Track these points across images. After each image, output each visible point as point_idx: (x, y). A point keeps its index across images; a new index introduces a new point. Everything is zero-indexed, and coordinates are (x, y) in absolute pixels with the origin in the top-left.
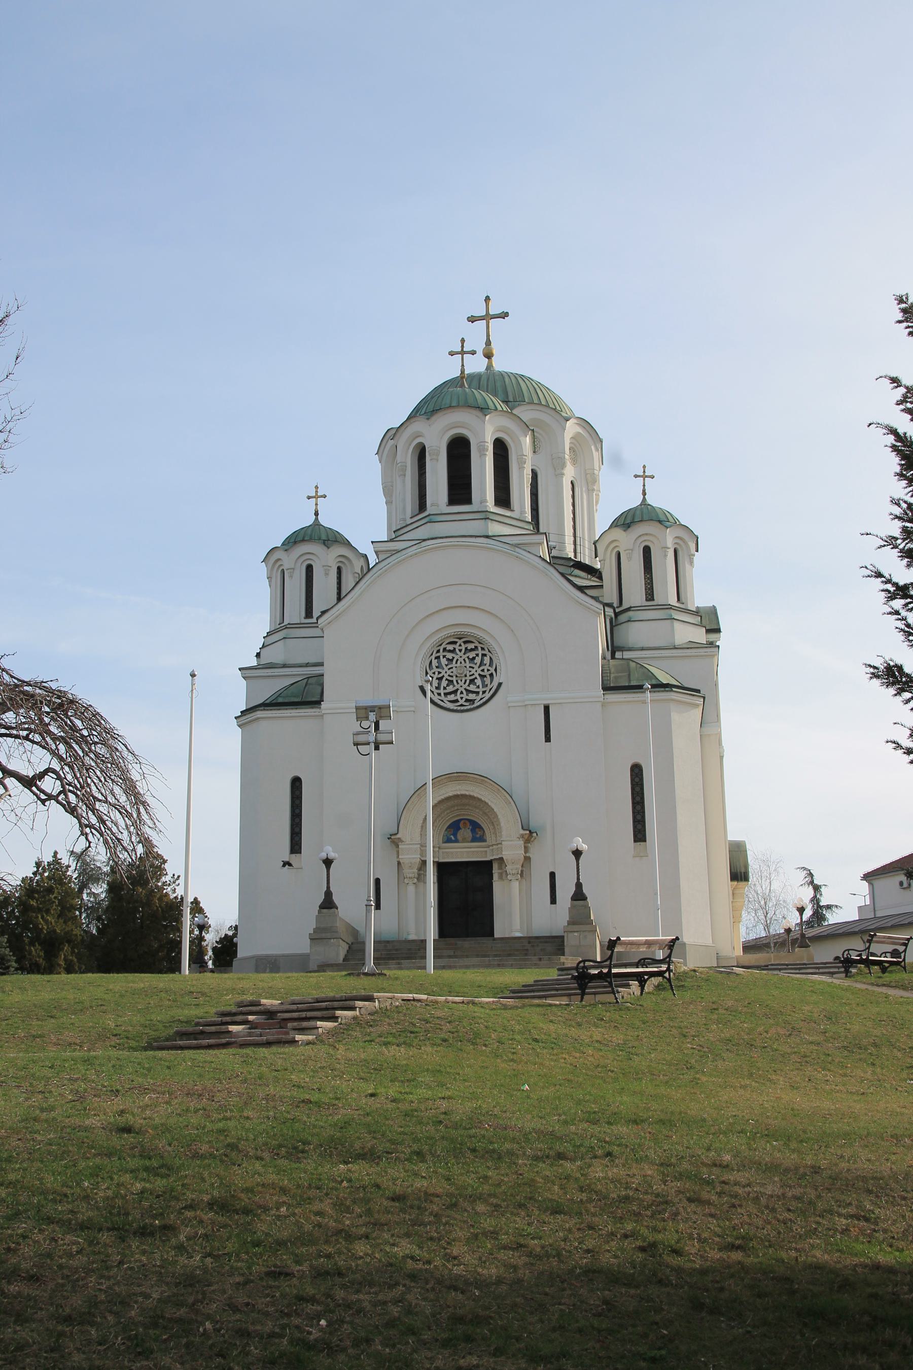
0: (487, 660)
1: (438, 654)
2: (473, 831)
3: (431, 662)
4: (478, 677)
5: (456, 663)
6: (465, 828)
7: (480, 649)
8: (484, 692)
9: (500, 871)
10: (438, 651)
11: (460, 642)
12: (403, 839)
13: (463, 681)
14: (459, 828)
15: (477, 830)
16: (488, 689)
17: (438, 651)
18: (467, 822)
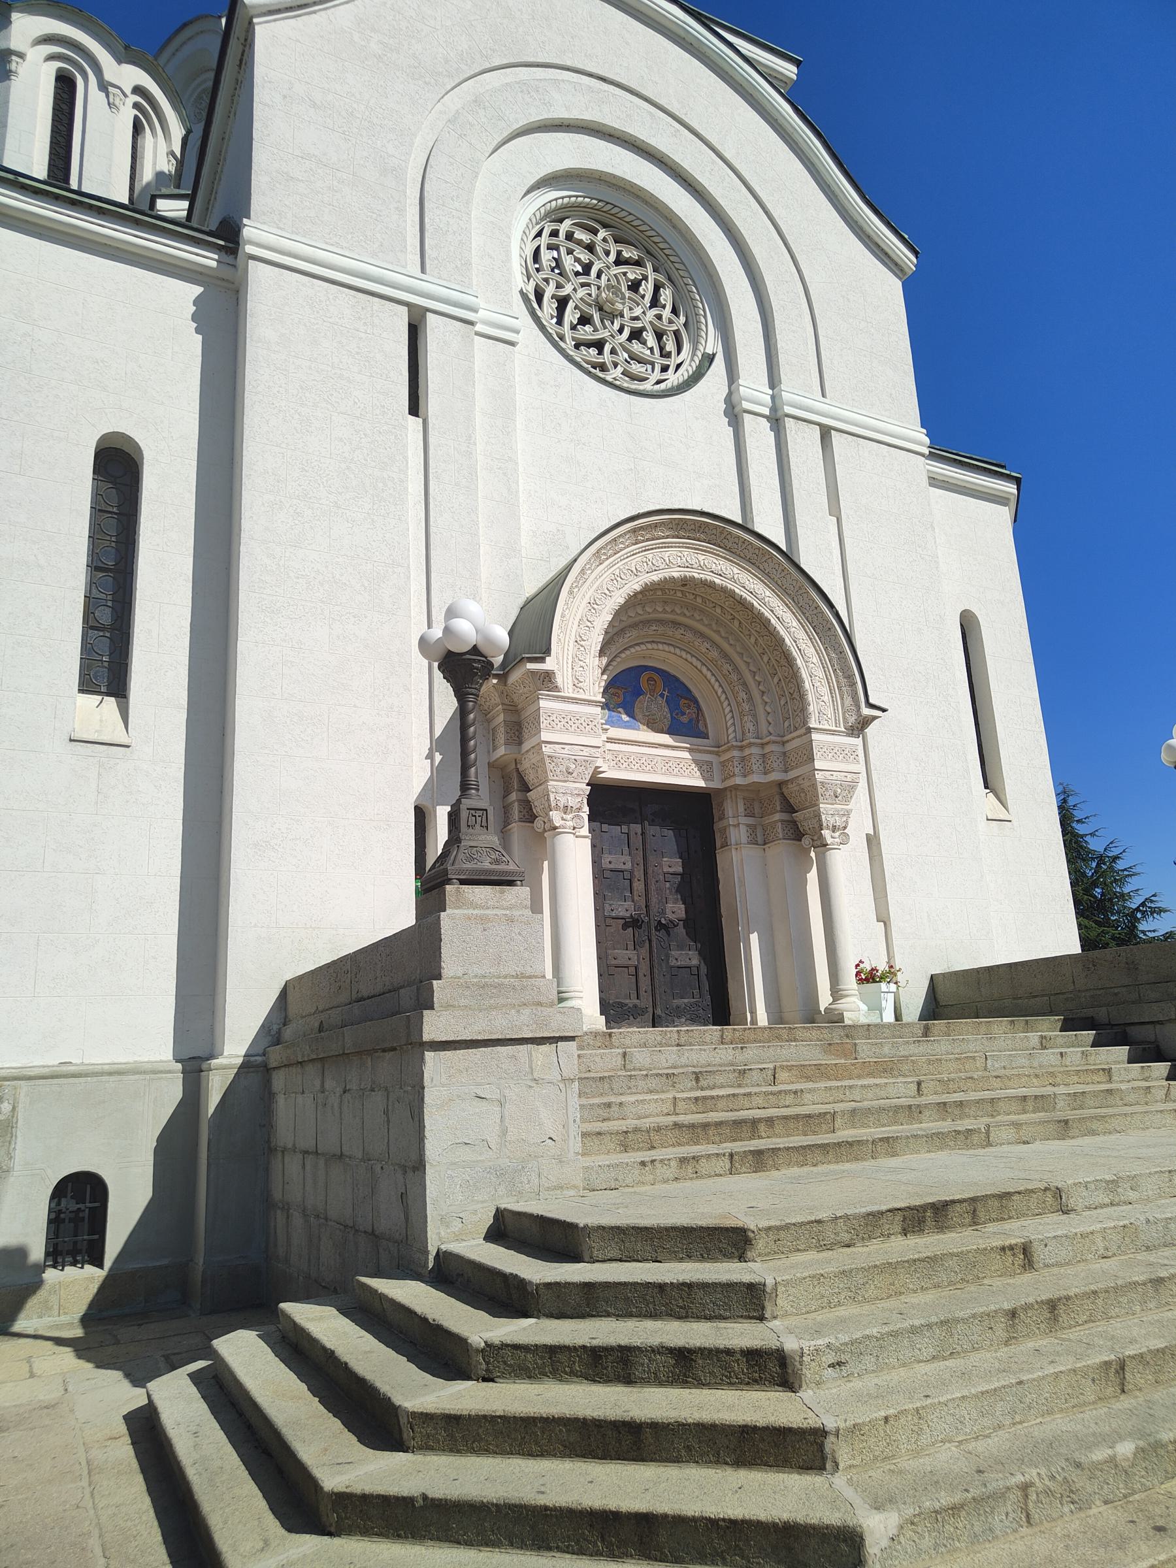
0: (666, 296)
1: (554, 241)
2: (672, 704)
3: (538, 248)
4: (649, 327)
5: (599, 276)
6: (652, 692)
7: (649, 266)
8: (665, 369)
9: (750, 821)
10: (554, 234)
11: (602, 233)
12: (558, 680)
13: (616, 326)
14: (638, 692)
15: (683, 701)
16: (673, 362)
17: (554, 234)
18: (656, 676)
